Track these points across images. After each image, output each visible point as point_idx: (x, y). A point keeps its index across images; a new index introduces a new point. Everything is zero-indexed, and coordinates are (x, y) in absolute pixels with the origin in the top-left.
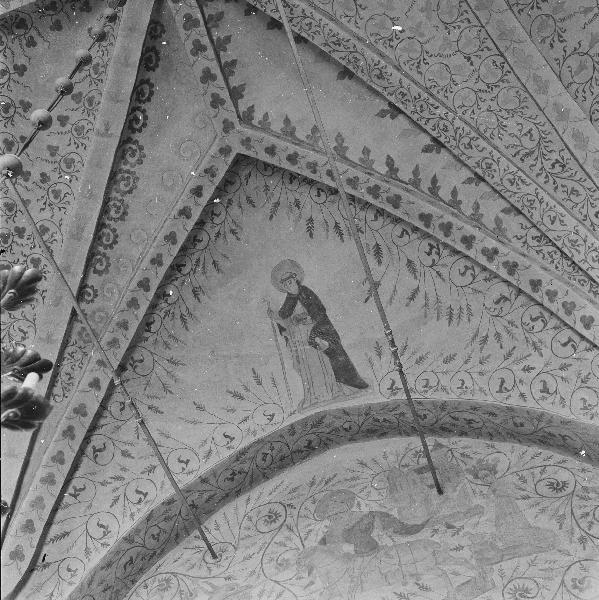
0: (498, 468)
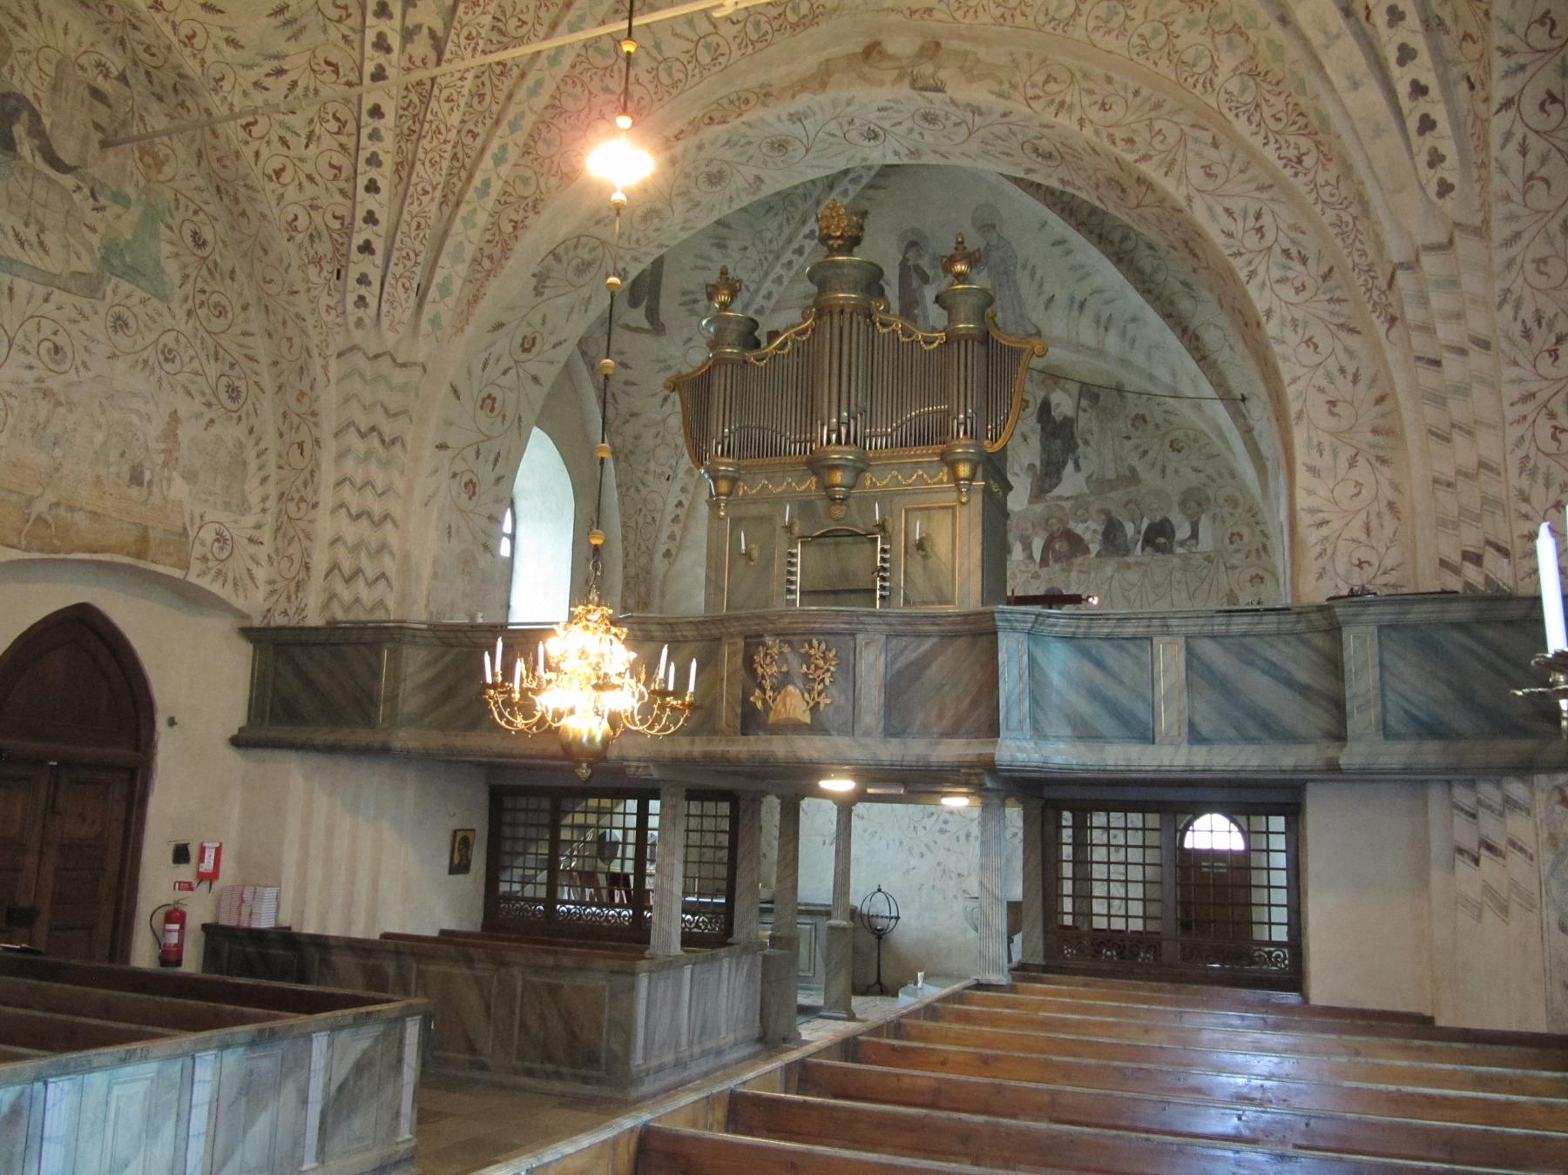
0: (166, 169)
